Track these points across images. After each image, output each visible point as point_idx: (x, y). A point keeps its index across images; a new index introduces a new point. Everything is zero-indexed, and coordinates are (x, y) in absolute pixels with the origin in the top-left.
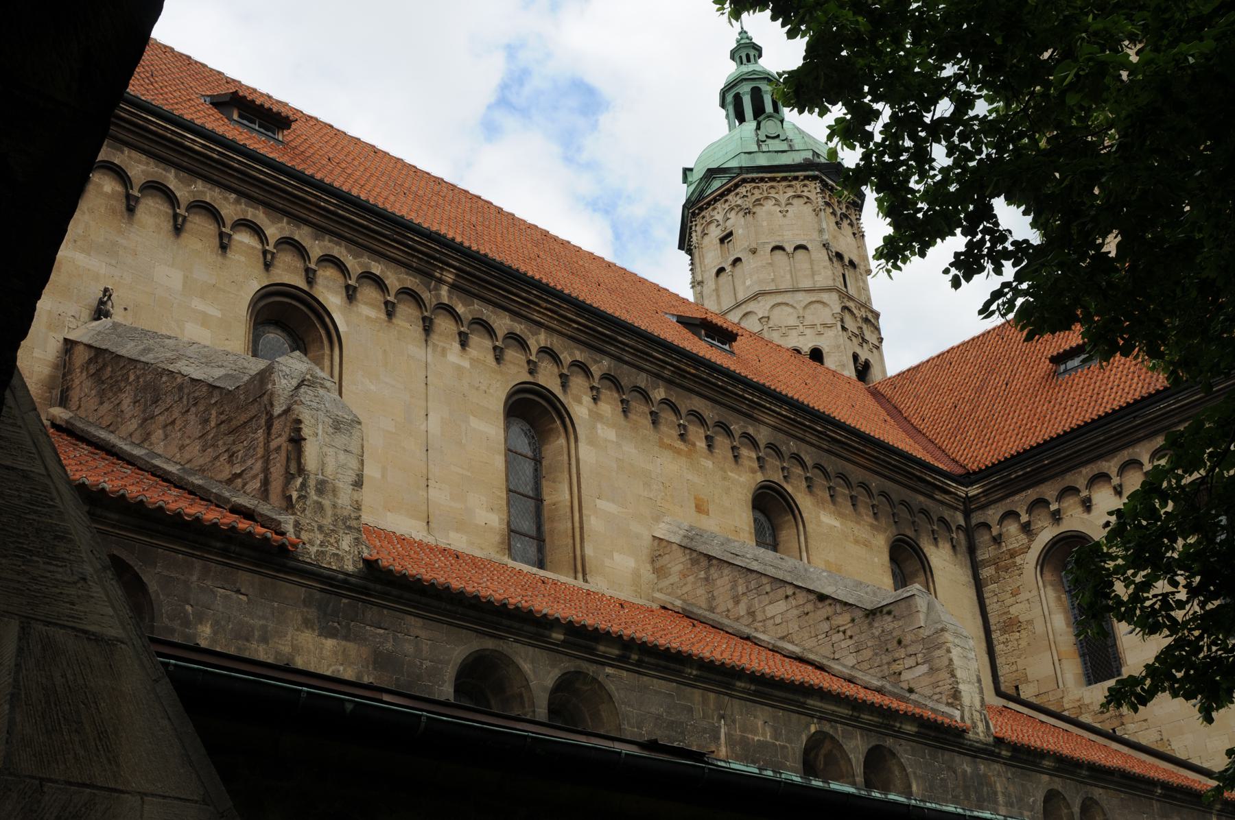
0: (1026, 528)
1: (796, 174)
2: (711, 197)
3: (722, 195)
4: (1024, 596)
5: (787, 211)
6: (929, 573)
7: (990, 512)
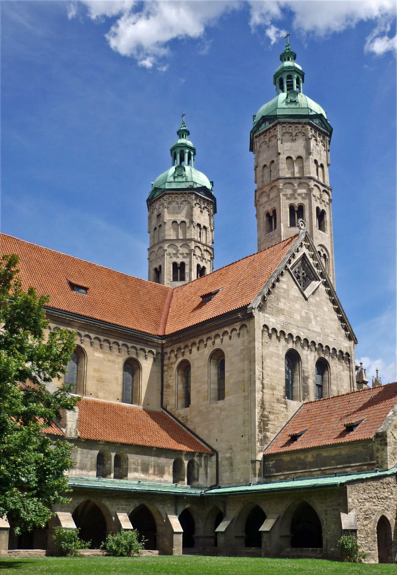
0: (176, 356)
4: (172, 378)
7: (168, 349)
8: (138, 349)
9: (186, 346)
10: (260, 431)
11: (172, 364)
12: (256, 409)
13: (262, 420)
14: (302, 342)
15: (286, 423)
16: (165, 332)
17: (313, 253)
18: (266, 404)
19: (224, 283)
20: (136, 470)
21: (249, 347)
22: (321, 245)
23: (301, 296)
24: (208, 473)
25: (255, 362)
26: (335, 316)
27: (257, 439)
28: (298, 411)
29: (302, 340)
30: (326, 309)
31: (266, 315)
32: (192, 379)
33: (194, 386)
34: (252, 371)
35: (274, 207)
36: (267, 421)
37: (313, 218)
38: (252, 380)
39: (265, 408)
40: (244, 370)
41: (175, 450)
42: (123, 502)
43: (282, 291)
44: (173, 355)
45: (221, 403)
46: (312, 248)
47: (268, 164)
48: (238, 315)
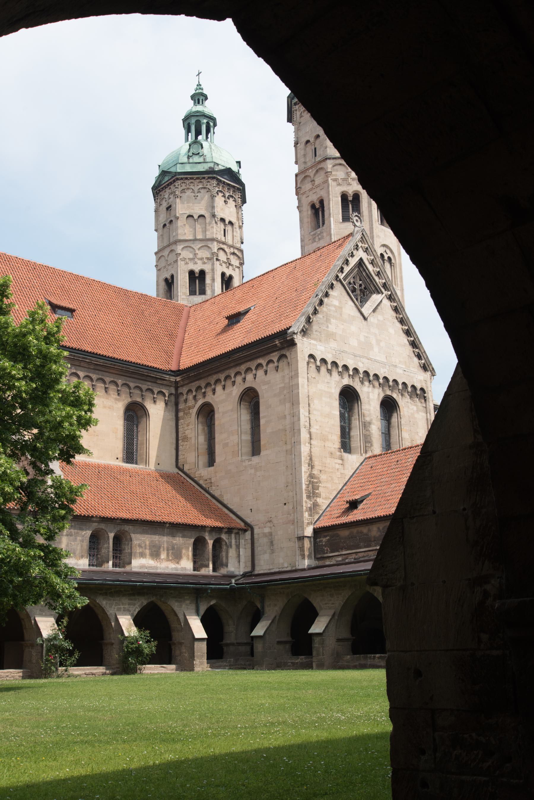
1: (204, 176)
2: (164, 185)
3: (168, 185)
4: (190, 427)
5: (198, 196)
6: (148, 417)
7: (184, 388)
8: (144, 389)
9: (208, 385)
10: (308, 497)
11: (190, 408)
12: (303, 468)
13: (310, 481)
14: (361, 376)
15: (343, 485)
16: (179, 366)
17: (372, 258)
18: (316, 460)
19: (256, 299)
20: (142, 555)
21: (291, 384)
22: (384, 246)
23: (359, 315)
24: (241, 556)
25: (299, 404)
26: (404, 340)
27: (304, 508)
28: (358, 468)
29: (361, 372)
30: (392, 331)
31: (313, 342)
32: (217, 428)
33: (219, 437)
34: (295, 416)
35: (321, 197)
36: (317, 483)
37: (373, 209)
38: (296, 428)
39: (314, 465)
40: (285, 416)
41: (195, 525)
42: (125, 600)
43: (333, 309)
44: (191, 397)
45: (256, 460)
46: (372, 251)
47: (312, 140)
48: (275, 342)
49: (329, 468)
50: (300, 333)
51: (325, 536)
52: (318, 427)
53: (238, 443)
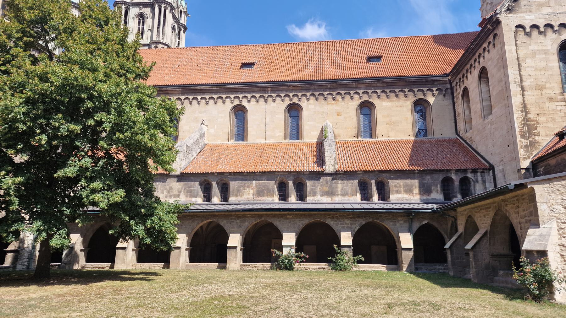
10: (523, 137)
13: (524, 125)
27: (519, 146)
31: (520, 15)
36: (534, 124)
44: (458, 87)
48: (488, 26)
49: (549, 111)
50: (506, 11)
51: (542, 167)
52: (532, 80)
53: (481, 109)
